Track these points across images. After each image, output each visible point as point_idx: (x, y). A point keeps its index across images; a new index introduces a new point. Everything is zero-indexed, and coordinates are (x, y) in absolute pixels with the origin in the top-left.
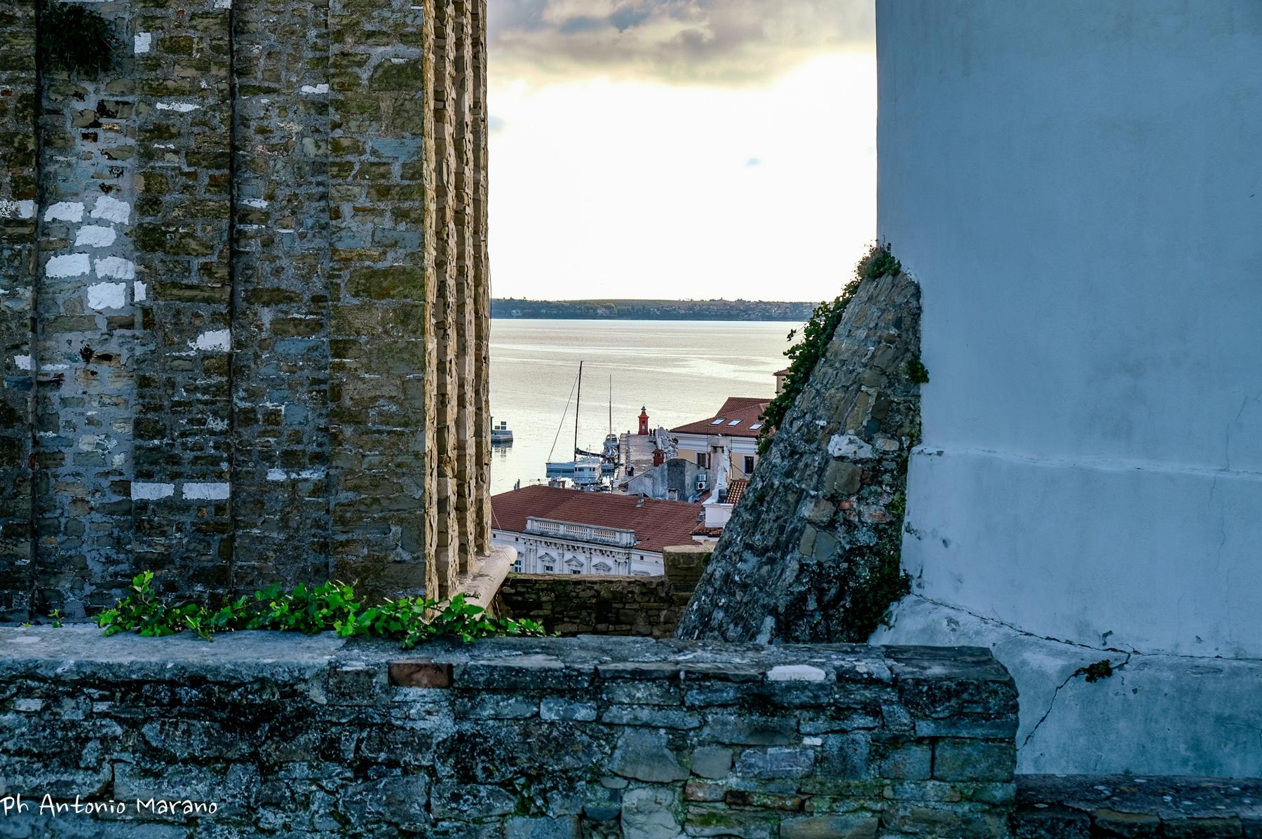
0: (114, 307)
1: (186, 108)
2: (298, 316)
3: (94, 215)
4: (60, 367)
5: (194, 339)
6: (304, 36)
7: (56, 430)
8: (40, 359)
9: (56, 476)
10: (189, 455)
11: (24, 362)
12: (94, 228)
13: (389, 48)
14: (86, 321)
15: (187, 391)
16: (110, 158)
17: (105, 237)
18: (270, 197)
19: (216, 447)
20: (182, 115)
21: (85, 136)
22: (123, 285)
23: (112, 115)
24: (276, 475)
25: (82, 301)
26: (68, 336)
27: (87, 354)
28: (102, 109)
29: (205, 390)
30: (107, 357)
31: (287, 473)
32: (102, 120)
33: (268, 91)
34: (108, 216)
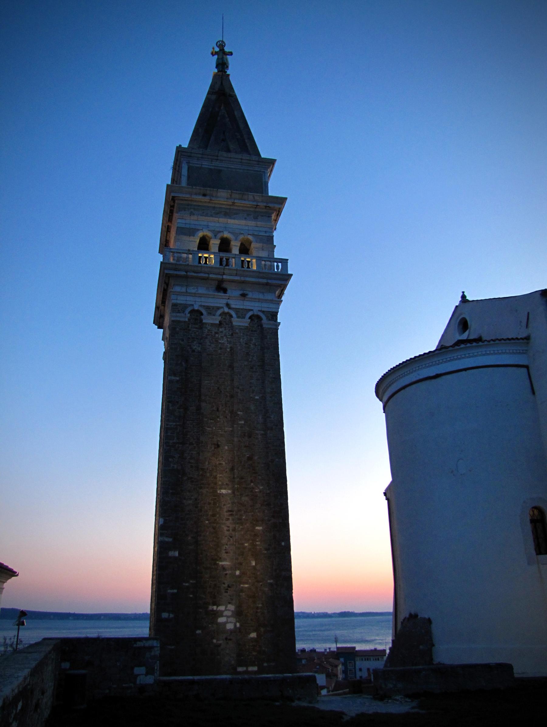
0: (232, 628)
1: (246, 586)
8: (218, 640)
11: (215, 641)
17: (229, 613)
22: (233, 624)
24: (265, 664)
25: (225, 627)
27: (226, 639)
28: (229, 586)
30: (230, 640)
32: (228, 588)
34: (230, 609)
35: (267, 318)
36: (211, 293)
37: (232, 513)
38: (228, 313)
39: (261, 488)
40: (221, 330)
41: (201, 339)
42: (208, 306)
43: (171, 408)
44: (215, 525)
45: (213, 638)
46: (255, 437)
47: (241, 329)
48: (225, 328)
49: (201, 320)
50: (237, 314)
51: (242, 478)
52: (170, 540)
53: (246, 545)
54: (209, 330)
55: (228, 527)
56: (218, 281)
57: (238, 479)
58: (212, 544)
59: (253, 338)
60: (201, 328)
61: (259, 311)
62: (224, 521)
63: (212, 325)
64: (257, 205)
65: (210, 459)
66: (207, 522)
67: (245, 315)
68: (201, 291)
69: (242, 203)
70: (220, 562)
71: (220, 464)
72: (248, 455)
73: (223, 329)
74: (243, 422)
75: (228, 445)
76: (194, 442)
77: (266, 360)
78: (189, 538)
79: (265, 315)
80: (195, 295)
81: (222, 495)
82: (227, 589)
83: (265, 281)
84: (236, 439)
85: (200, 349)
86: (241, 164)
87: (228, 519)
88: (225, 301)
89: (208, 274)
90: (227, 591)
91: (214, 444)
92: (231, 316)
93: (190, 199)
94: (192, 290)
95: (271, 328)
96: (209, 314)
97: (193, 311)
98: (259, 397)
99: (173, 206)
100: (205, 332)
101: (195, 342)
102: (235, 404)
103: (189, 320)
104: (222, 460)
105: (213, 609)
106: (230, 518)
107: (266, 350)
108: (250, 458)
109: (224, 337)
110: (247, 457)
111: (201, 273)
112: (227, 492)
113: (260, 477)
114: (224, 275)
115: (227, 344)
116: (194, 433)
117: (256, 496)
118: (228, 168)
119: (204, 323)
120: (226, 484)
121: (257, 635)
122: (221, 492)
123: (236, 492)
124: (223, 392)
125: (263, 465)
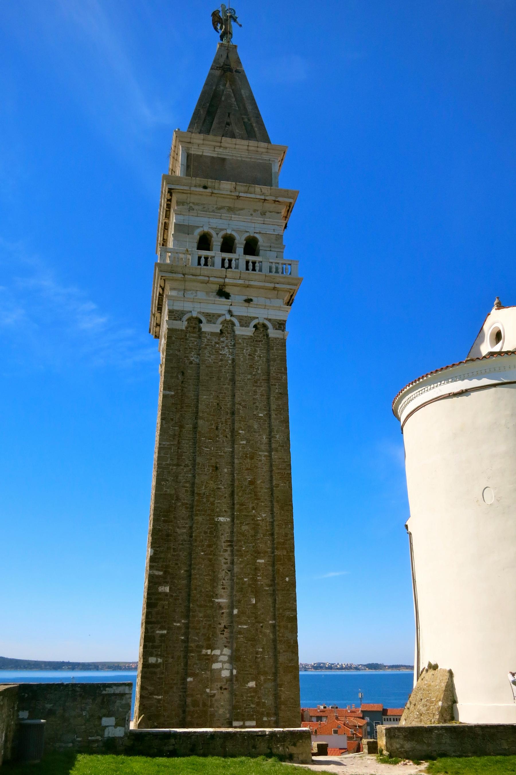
1: (245, 627)
2: (270, 678)
3: (223, 653)
4: (215, 692)
5: (247, 684)
6: (270, 609)
7: (214, 708)
9: (213, 720)
10: (246, 714)
11: (208, 690)
13: (290, 613)
14: (221, 679)
15: (246, 697)
18: (263, 648)
19: (252, 712)
20: (245, 628)
21: (221, 634)
22: (229, 671)
24: (265, 719)
25: (220, 675)
26: (216, 684)
27: (221, 688)
28: (225, 627)
29: (250, 697)
30: (226, 689)
31: (268, 718)
33: (262, 622)
35: (273, 327)
36: (212, 298)
38: (230, 321)
39: (264, 515)
40: (222, 339)
41: (200, 350)
42: (208, 313)
43: (165, 426)
44: (211, 557)
45: (207, 687)
46: (258, 459)
47: (245, 339)
48: (227, 337)
49: (200, 329)
50: (240, 322)
51: (242, 505)
52: (161, 573)
53: (245, 580)
55: (226, 559)
56: (219, 285)
58: (207, 579)
59: (258, 349)
60: (200, 337)
61: (265, 319)
62: (222, 553)
63: (213, 334)
64: (265, 200)
65: (207, 483)
66: (202, 553)
67: (249, 323)
69: (247, 196)
70: (216, 599)
71: (219, 488)
72: (249, 478)
74: (245, 442)
75: (227, 467)
77: (272, 374)
79: (272, 323)
81: (221, 523)
82: (224, 631)
83: (272, 285)
84: (236, 461)
85: (197, 361)
86: (247, 151)
87: (226, 551)
88: (227, 308)
89: (208, 276)
90: (223, 632)
91: (212, 466)
92: (233, 324)
93: (189, 192)
95: (278, 338)
96: (209, 322)
99: (169, 200)
100: (204, 342)
102: (236, 422)
103: (187, 328)
104: (221, 485)
105: (207, 653)
106: (229, 549)
107: (272, 363)
108: (252, 483)
110: (249, 480)
111: (200, 275)
112: (225, 521)
113: (263, 504)
114: (225, 278)
115: (229, 355)
116: (189, 453)
117: (258, 525)
119: (203, 332)
120: (225, 511)
121: (256, 685)
122: (219, 520)
123: (235, 520)
124: (223, 408)
125: (266, 491)
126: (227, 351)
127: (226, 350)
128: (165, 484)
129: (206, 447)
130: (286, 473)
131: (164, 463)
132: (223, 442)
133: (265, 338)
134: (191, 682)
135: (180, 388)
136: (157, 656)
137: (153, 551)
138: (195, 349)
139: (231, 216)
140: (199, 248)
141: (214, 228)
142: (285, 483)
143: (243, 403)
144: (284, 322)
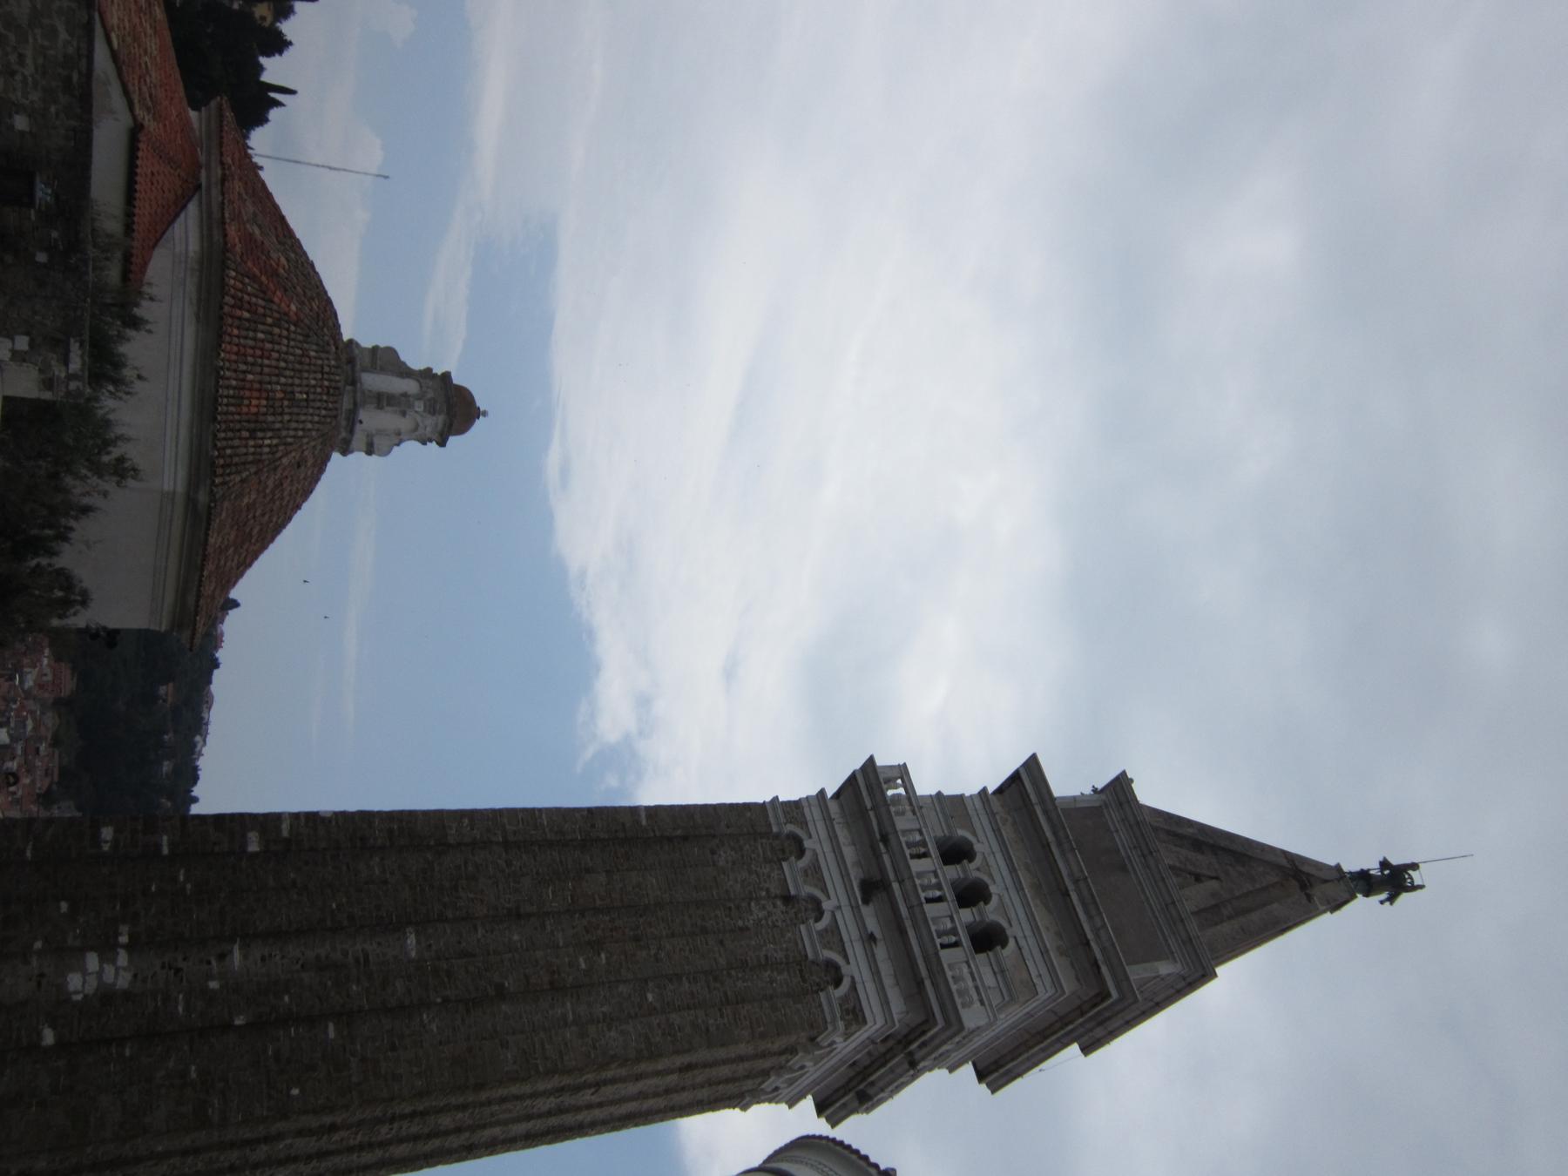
1: (180, 1009)
3: (122, 973)
4: (34, 962)
5: (50, 1026)
11: (38, 945)
12: (113, 971)
13: (217, 1106)
16: (152, 977)
17: (109, 973)
20: (176, 1007)
21: (164, 963)
23: (175, 974)
27: (42, 975)
28: (178, 970)
30: (39, 984)
32: (172, 971)
37: (362, 960)
40: (779, 903)
42: (819, 867)
47: (797, 944)
50: (826, 930)
52: (285, 833)
53: (286, 998)
54: (769, 877)
57: (445, 966)
59: (785, 975)
61: (853, 978)
64: (1088, 943)
66: (334, 906)
67: (831, 949)
68: (849, 853)
73: (783, 908)
74: (583, 966)
76: (513, 868)
78: (292, 875)
80: (833, 838)
82: (170, 968)
83: (924, 972)
84: (539, 954)
85: (721, 863)
94: (842, 834)
95: (823, 1011)
97: (798, 842)
98: (651, 1003)
100: (761, 868)
101: (733, 853)
103: (777, 836)
104: (484, 931)
105: (121, 934)
108: (501, 993)
109: (765, 913)
118: (1140, 883)
119: (781, 865)
120: (430, 946)
124: (641, 920)
126: (760, 916)
127: (762, 914)
128: (465, 825)
129: (553, 892)
130: (539, 1061)
131: (506, 821)
132: (574, 928)
133: (814, 988)
134: (59, 908)
135: (658, 834)
136: (115, 843)
137: (329, 815)
138: (743, 856)
139: (1024, 886)
140: (940, 844)
141: (986, 861)
142: (515, 1063)
143: (662, 955)
144: (860, 1019)
